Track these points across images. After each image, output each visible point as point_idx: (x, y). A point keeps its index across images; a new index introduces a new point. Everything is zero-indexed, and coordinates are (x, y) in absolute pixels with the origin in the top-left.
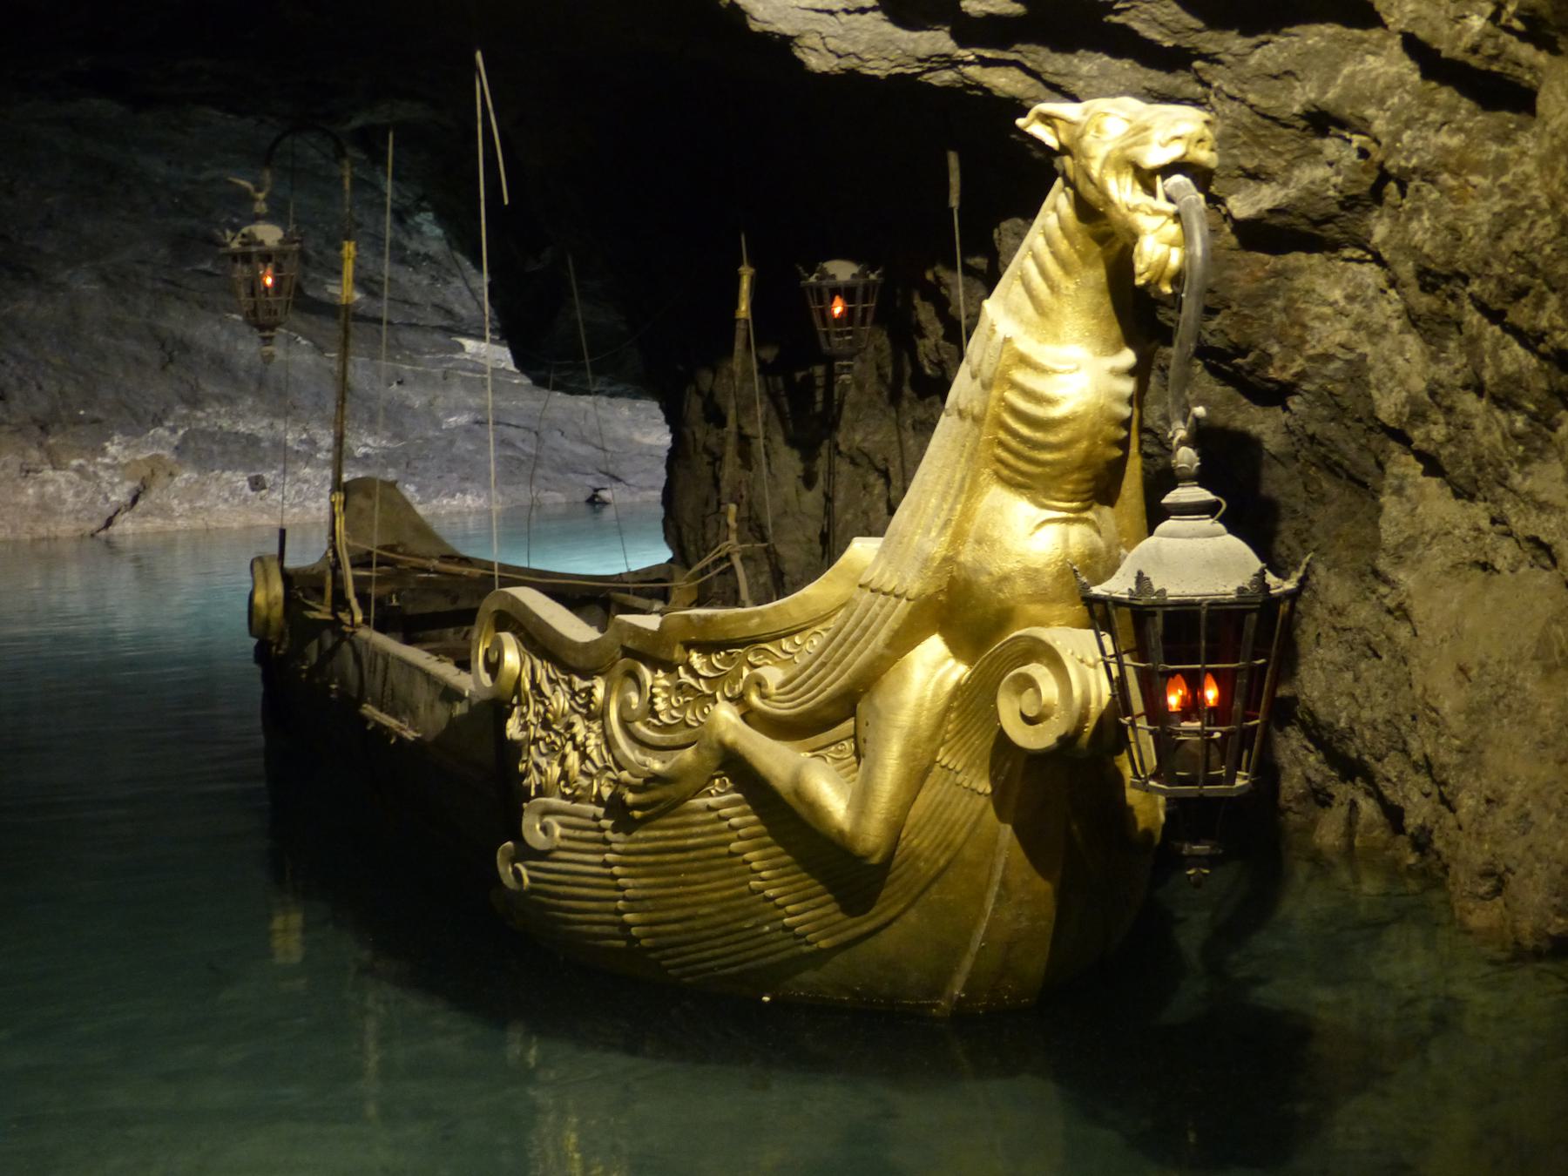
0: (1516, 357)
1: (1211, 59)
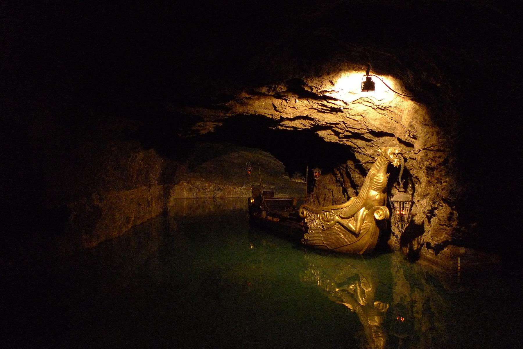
1: (374, 141)
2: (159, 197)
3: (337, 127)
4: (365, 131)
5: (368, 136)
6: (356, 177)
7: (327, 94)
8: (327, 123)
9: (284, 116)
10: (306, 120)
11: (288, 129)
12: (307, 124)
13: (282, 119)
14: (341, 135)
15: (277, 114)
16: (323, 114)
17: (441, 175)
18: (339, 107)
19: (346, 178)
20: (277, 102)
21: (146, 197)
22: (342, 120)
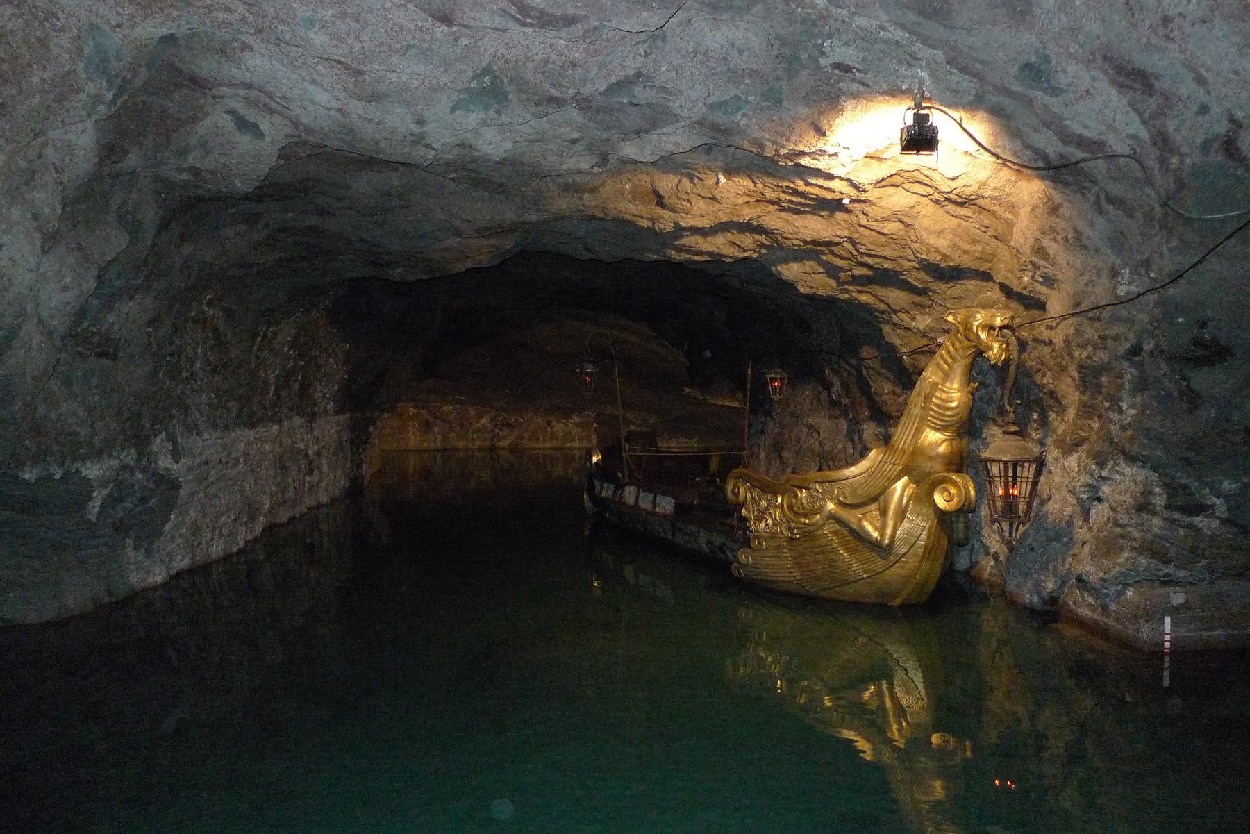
1: (934, 292)
2: (340, 447)
3: (833, 253)
4: (909, 263)
5: (919, 278)
6: (886, 391)
7: (806, 161)
8: (805, 242)
9: (686, 222)
10: (748, 234)
11: (697, 258)
13: (679, 231)
15: (666, 217)
16: (795, 216)
18: (836, 196)
21: (302, 446)
22: (846, 233)
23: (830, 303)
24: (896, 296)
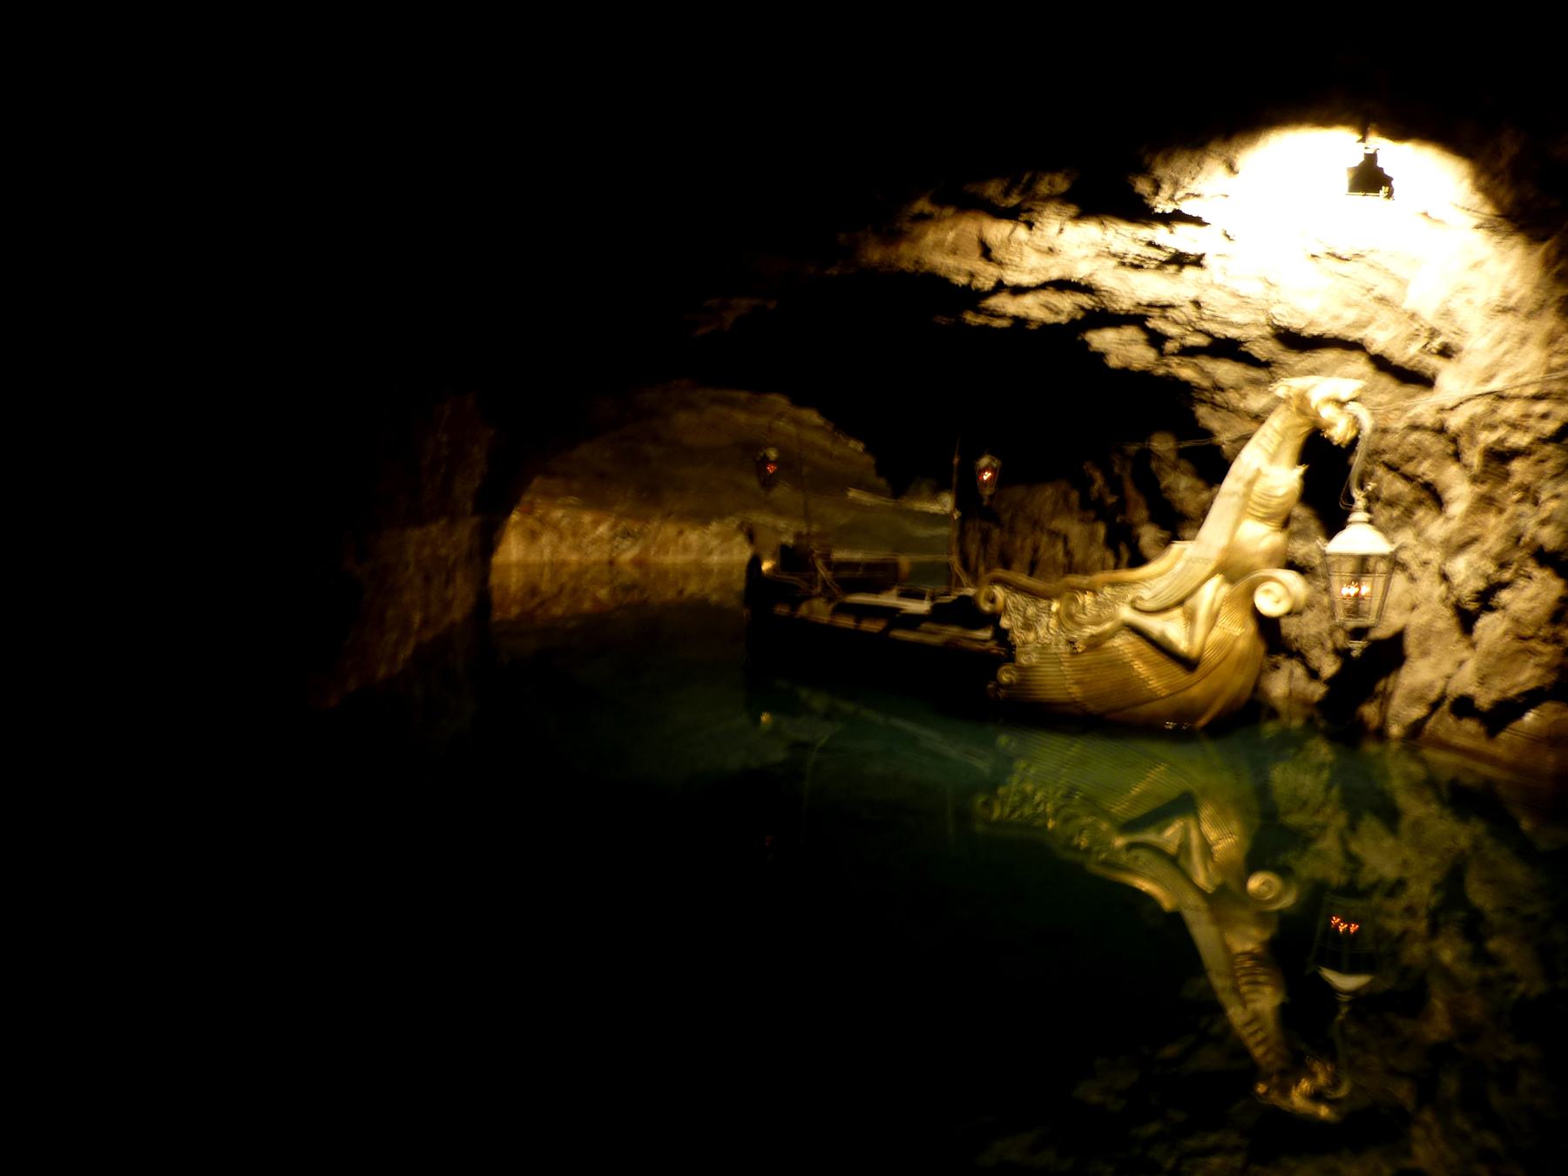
0: (1400, 486)
9: (1012, 277)
11: (998, 323)
12: (1067, 304)
13: (1000, 287)
14: (1170, 346)
17: (1541, 476)
19: (1130, 490)
20: (997, 231)
23: (1144, 377)
24: (1225, 371)
